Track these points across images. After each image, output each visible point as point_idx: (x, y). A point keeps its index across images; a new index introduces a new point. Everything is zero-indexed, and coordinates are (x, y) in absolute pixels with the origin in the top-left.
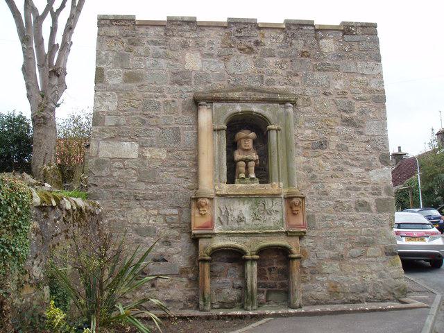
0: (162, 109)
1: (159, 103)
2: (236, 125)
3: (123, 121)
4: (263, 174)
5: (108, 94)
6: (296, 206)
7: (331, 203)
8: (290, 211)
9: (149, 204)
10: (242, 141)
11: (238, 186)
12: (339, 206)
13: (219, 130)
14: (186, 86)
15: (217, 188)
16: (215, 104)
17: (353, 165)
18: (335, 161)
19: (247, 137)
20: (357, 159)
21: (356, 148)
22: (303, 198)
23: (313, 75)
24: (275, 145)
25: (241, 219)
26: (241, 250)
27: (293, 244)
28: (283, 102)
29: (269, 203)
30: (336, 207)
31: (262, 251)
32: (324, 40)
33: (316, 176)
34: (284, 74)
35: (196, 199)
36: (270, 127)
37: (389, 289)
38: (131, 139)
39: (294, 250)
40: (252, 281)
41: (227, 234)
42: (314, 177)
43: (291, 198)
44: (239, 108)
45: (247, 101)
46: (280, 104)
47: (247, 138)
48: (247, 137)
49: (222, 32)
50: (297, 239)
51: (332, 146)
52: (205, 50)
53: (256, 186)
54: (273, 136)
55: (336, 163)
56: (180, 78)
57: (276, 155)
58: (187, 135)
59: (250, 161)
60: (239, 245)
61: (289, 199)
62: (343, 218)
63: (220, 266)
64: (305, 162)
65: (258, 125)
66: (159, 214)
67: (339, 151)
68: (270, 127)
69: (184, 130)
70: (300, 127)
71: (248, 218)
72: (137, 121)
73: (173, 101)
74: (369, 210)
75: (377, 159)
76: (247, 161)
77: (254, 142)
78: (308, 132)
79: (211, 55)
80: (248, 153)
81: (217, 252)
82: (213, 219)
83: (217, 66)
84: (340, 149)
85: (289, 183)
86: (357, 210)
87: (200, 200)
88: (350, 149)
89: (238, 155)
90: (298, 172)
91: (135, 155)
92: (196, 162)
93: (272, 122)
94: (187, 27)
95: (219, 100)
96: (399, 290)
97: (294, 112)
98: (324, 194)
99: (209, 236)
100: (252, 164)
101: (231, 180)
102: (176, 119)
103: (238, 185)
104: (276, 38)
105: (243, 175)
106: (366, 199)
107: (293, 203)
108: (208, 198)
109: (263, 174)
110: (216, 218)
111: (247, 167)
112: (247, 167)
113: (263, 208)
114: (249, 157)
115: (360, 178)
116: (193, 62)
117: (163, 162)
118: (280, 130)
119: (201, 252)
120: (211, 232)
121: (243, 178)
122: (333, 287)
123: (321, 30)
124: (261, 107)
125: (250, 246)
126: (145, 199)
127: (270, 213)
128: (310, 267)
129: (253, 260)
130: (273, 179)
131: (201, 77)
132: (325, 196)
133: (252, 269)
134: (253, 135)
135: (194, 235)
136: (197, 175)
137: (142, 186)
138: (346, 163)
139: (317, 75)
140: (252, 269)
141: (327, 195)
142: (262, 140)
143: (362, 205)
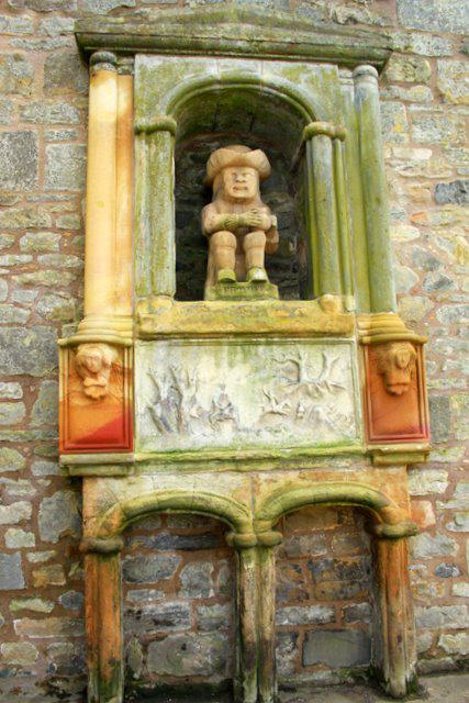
2: (210, 123)
4: (293, 272)
6: (398, 367)
8: (377, 383)
10: (228, 174)
11: (214, 308)
13: (150, 132)
15: (143, 312)
16: (141, 60)
22: (418, 344)
24: (330, 183)
25: (221, 414)
28: (348, 61)
29: (308, 355)
31: (293, 516)
33: (450, 283)
35: (72, 347)
36: (312, 125)
39: (394, 508)
40: (259, 614)
41: (176, 461)
43: (386, 343)
44: (215, 69)
46: (341, 65)
47: (241, 164)
48: (242, 169)
50: (402, 471)
53: (271, 308)
54: (322, 151)
57: (333, 212)
59: (251, 229)
61: (375, 347)
64: (416, 241)
65: (275, 127)
68: (312, 125)
69: (46, 141)
70: (398, 140)
71: (247, 415)
73: (17, 58)
76: (241, 231)
77: (264, 185)
81: (139, 523)
87: (83, 350)
89: (213, 215)
90: (401, 274)
92: (77, 238)
95: (154, 47)
97: (382, 98)
99: (115, 470)
100: (257, 244)
101: (191, 284)
102: (22, 108)
103: (211, 303)
108: (112, 344)
109: (293, 272)
110: (140, 408)
111: (241, 251)
113: (294, 379)
114: (246, 216)
118: (342, 138)
119: (92, 528)
121: (229, 282)
124: (284, 73)
125: (244, 499)
127: (314, 393)
129: (263, 547)
130: (327, 283)
134: (258, 157)
135: (66, 467)
136: (80, 275)
140: (260, 573)
142: (289, 176)
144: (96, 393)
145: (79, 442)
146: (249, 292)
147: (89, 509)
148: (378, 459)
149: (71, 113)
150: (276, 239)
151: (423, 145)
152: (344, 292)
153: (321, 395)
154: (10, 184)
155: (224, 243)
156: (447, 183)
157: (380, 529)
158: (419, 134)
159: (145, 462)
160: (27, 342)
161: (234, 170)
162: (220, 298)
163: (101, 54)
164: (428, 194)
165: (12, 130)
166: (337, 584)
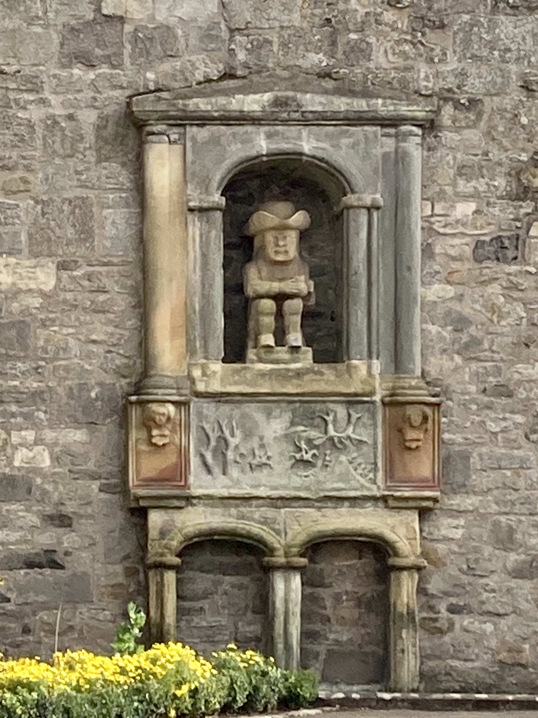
9: (13, 415)
14: (105, 70)
19: (281, 225)
23: (492, 26)
26: (261, 541)
27: (400, 530)
34: (403, 24)
58: (114, 222)
60: (256, 529)
63: (202, 582)
66: (38, 441)
76: (280, 298)
80: (283, 273)
82: (183, 454)
85: (398, 361)
99: (176, 503)
105: (268, 339)
111: (279, 315)
112: (279, 315)
114: (288, 287)
128: (447, 594)
144: (160, 442)
145: (145, 480)
146: (287, 356)
149: (124, 178)
150: (312, 301)
151: (466, 197)
156: (487, 239)
157: (392, 561)
158: (463, 186)
159: (199, 498)
160: (93, 395)
164: (468, 251)
166: (356, 613)
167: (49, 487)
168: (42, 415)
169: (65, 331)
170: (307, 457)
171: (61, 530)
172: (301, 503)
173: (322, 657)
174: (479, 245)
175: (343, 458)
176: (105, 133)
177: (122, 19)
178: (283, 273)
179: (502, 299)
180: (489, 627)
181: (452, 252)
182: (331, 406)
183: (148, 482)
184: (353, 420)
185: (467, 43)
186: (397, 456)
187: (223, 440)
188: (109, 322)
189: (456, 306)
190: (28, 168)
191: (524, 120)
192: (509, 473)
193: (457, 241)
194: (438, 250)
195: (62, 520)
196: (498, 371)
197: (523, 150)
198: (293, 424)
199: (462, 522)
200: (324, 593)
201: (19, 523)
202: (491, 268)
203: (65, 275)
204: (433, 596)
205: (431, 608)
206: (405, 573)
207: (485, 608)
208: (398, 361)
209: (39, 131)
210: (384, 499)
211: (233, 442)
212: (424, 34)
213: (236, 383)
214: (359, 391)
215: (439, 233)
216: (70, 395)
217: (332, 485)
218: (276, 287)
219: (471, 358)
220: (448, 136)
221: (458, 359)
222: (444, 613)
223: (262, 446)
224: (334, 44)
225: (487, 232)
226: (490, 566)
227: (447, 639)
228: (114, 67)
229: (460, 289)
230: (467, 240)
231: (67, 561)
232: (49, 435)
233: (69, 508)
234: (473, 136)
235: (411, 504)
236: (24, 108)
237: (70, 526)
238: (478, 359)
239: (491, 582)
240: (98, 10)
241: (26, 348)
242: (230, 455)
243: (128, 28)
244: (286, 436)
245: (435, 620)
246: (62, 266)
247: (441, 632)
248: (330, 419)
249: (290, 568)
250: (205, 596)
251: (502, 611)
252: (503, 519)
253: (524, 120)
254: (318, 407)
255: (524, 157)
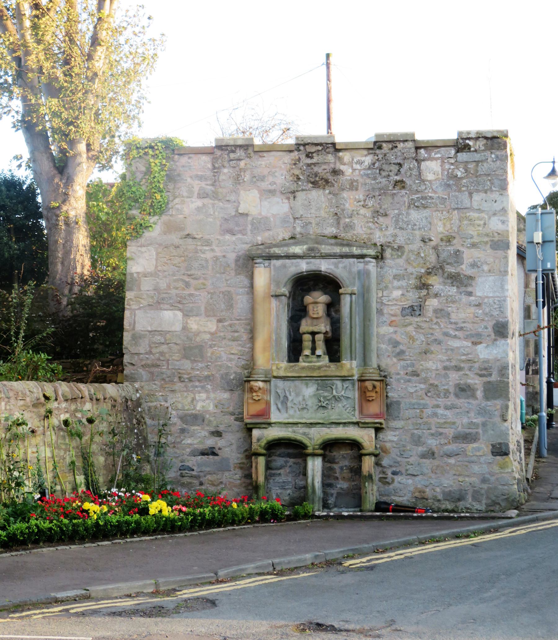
0: (210, 267)
1: (207, 261)
3: (163, 285)
5: (144, 249)
7: (422, 386)
9: (197, 387)
12: (432, 389)
14: (240, 236)
16: (274, 262)
17: (455, 337)
18: (431, 331)
19: (317, 301)
20: (461, 329)
21: (462, 313)
23: (408, 214)
26: (301, 443)
27: (366, 437)
30: (429, 392)
31: (329, 446)
32: (428, 163)
34: (369, 214)
36: (341, 291)
37: (494, 498)
38: (173, 307)
40: (313, 480)
42: (402, 352)
44: (304, 266)
45: (314, 257)
49: (288, 158)
51: (429, 313)
52: (264, 185)
55: (432, 334)
56: (236, 221)
58: (241, 302)
60: (299, 437)
62: (438, 406)
63: (279, 461)
65: (330, 284)
66: (208, 398)
67: (437, 318)
72: (181, 284)
74: (474, 396)
75: (490, 329)
76: (313, 334)
78: (397, 294)
79: (272, 192)
80: (316, 323)
81: (274, 446)
82: (268, 404)
83: (278, 207)
84: (438, 315)
85: (365, 361)
86: (457, 395)
88: (453, 316)
89: (305, 326)
91: (178, 327)
93: (348, 282)
94: (240, 153)
96: (507, 499)
98: (414, 375)
99: (264, 426)
100: (320, 338)
102: (227, 280)
104: (360, 163)
105: (307, 352)
106: (470, 381)
107: (373, 388)
108: (262, 381)
111: (314, 341)
112: (314, 341)
114: (316, 329)
115: (464, 355)
116: (250, 201)
117: (212, 334)
118: (355, 294)
119: (255, 446)
120: (269, 421)
121: (307, 356)
122: (420, 492)
123: (425, 148)
126: (191, 381)
128: (391, 466)
130: (343, 357)
131: (261, 224)
132: (415, 378)
133: (315, 466)
135: (246, 424)
137: (187, 365)
138: (446, 334)
139: (414, 215)
140: (315, 466)
141: (418, 375)
143: (464, 390)
144: (257, 398)
147: (254, 440)
148: (360, 425)
149: (246, 282)
150: (330, 335)
151: (398, 288)
152: (351, 360)
153: (341, 400)
154: (224, 313)
155: (307, 338)
156: (407, 306)
157: (363, 452)
158: (396, 283)
159: (274, 423)
160: (232, 377)
161: (313, 305)
162: (304, 362)
163: (258, 261)
164: (399, 312)
165: (223, 290)
166: (350, 475)
167: (212, 419)
168: (209, 387)
169: (220, 349)
170: (324, 405)
171: (217, 438)
172: (320, 425)
173: (335, 495)
174: (404, 309)
175: (340, 405)
176: (238, 263)
177: (247, 215)
178: (316, 323)
179: (414, 333)
180: (410, 481)
181: (392, 312)
182: (335, 382)
183: (253, 416)
184: (345, 387)
185: (397, 221)
186: (364, 404)
187: (286, 397)
188: (240, 345)
189: (394, 336)
190: (205, 279)
191: (422, 255)
192: (418, 411)
193: (394, 308)
194: (385, 311)
195: (218, 434)
196: (413, 365)
197: (422, 267)
198: (317, 390)
199: (397, 433)
200: (336, 466)
201: (199, 435)
202: (410, 319)
203: (220, 325)
204: (384, 467)
205: (384, 473)
206: (367, 457)
207: (409, 472)
208: (365, 361)
209: (210, 262)
210: (357, 424)
211: (290, 398)
212: (378, 219)
213: (291, 372)
214: (346, 375)
215: (385, 305)
216: (222, 377)
217: (334, 418)
218: (311, 329)
219: (400, 360)
220: (389, 262)
221: (395, 360)
222: (390, 475)
223: (304, 400)
224: (338, 223)
225: (407, 304)
226: (410, 453)
227: (391, 487)
228: (243, 235)
229: (396, 329)
230: (398, 307)
231: (219, 452)
232: (212, 395)
233: (221, 428)
234: (401, 261)
235: (369, 425)
236: (204, 253)
237: (221, 436)
238: (403, 360)
239: (411, 460)
240: (237, 211)
241: (202, 357)
242: (289, 404)
243: (250, 218)
244: (314, 395)
245: (386, 478)
246: (220, 321)
247: (389, 484)
248: (334, 387)
249: (314, 455)
250: (281, 468)
251: (415, 474)
252: (416, 432)
253: (422, 255)
254: (329, 382)
255: (423, 271)
